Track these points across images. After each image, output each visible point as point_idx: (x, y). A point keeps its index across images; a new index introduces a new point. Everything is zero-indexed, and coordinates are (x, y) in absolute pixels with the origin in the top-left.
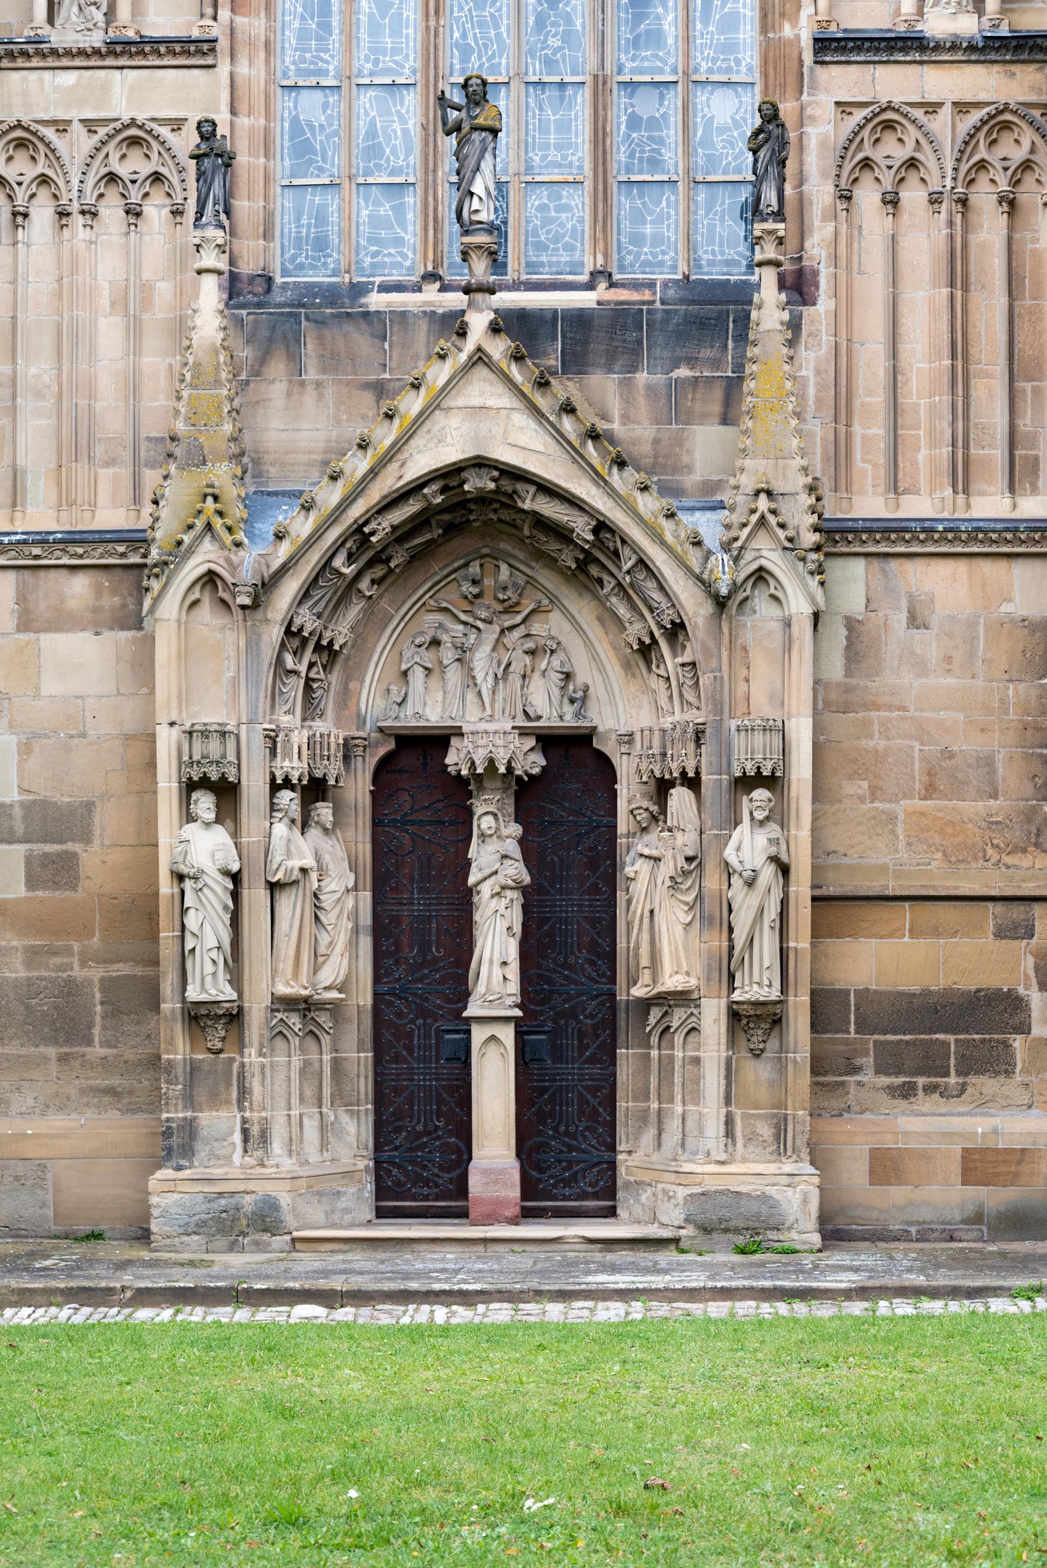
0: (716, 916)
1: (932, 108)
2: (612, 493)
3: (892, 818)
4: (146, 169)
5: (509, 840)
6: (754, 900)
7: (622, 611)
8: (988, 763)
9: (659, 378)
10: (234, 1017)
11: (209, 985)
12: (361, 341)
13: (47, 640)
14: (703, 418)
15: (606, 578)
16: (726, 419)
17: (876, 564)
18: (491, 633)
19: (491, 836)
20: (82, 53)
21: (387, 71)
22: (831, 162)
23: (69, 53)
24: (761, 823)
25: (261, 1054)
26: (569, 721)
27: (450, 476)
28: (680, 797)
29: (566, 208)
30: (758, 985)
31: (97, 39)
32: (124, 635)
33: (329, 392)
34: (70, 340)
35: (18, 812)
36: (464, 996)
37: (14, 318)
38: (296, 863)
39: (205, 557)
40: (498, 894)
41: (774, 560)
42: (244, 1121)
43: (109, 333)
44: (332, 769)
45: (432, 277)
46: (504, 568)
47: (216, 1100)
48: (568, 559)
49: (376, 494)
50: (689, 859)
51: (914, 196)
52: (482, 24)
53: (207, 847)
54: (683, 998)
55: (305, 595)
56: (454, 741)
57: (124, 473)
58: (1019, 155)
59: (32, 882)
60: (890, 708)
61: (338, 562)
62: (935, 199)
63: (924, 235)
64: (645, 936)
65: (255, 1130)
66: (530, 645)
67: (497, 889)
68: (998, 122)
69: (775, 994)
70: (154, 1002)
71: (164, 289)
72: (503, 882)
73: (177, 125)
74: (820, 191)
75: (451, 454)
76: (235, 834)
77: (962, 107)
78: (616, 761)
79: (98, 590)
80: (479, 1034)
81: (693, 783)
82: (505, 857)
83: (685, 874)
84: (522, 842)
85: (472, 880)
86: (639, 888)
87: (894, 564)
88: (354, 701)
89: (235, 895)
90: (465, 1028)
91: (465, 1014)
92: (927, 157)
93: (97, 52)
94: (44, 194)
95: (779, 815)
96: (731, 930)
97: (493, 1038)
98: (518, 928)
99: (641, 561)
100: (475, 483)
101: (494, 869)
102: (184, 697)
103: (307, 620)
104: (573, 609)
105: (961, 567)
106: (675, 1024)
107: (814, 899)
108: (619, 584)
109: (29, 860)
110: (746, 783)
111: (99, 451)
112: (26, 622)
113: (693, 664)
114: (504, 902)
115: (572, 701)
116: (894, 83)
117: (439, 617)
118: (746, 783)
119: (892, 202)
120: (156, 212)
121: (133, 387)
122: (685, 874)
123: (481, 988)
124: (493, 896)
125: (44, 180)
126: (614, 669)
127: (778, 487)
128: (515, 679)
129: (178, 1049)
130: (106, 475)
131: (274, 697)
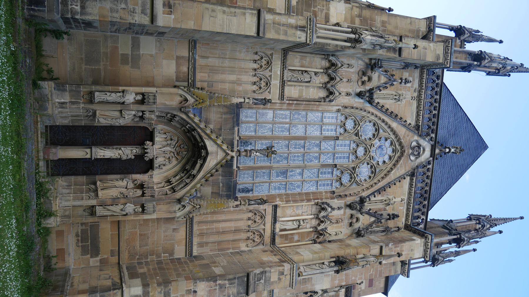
0: (115, 201)
1: (264, 225)
2: (201, 179)
3: (135, 228)
4: (262, 86)
6: (118, 211)
7: (177, 178)
8: (147, 245)
9: (220, 181)
10: (91, 101)
11: (98, 97)
12: (229, 126)
13: (174, 62)
14: (212, 189)
15: (184, 174)
16: (212, 193)
17: (185, 222)
18: (173, 150)
20: (283, 76)
21: (275, 129)
22: (256, 209)
23: (283, 73)
24: (134, 210)
25: (82, 107)
26: (156, 165)
27: (205, 147)
28: (139, 192)
29: (250, 161)
30: (100, 211)
31: (285, 79)
32: (175, 77)
33: (220, 120)
34: (232, 70)
35: (138, 53)
37: (236, 59)
38: (126, 116)
39: (191, 100)
41: (188, 209)
42: (66, 103)
43: (233, 77)
44: (146, 121)
45: (240, 138)
46: (186, 153)
47: (71, 96)
48: (188, 167)
49: (203, 134)
50: (127, 196)
51: (250, 222)
52: (282, 146)
53: (130, 98)
54: (97, 195)
55: (182, 119)
56: (151, 143)
57: (207, 79)
58: (256, 240)
59: (123, 55)
60: (157, 227)
61: (189, 125)
62: (249, 226)
63: (243, 225)
64: (110, 185)
65: (64, 106)
66: (171, 158)
68: (261, 236)
69: (97, 215)
70: (96, 82)
71: (241, 88)
73: (269, 92)
74: (251, 207)
75: (209, 148)
76: (132, 103)
77: (264, 230)
78: (147, 174)
79: (184, 73)
80: (88, 150)
81: (143, 195)
83: (124, 195)
84: (131, 159)
86: (120, 183)
87: (185, 225)
89: (119, 103)
92: (257, 224)
93: (283, 79)
94: (259, 66)
95: (136, 213)
96: (112, 205)
99: (187, 184)
100: (203, 153)
102: (162, 93)
103: (177, 119)
104: (178, 166)
105: (185, 237)
106: (91, 194)
107: (119, 221)
108: (182, 177)
109: (128, 54)
110: (143, 207)
111: (211, 74)
112: (178, 58)
113: (167, 194)
114: (117, 155)
116: (269, 219)
117: (176, 140)
118: (143, 207)
119: (249, 219)
120: (255, 88)
121: (223, 82)
122: (124, 195)
123: (99, 150)
125: (261, 66)
126: (165, 174)
127: (201, 209)
128: (164, 155)
129: (83, 89)
130: (206, 75)
131: (162, 112)
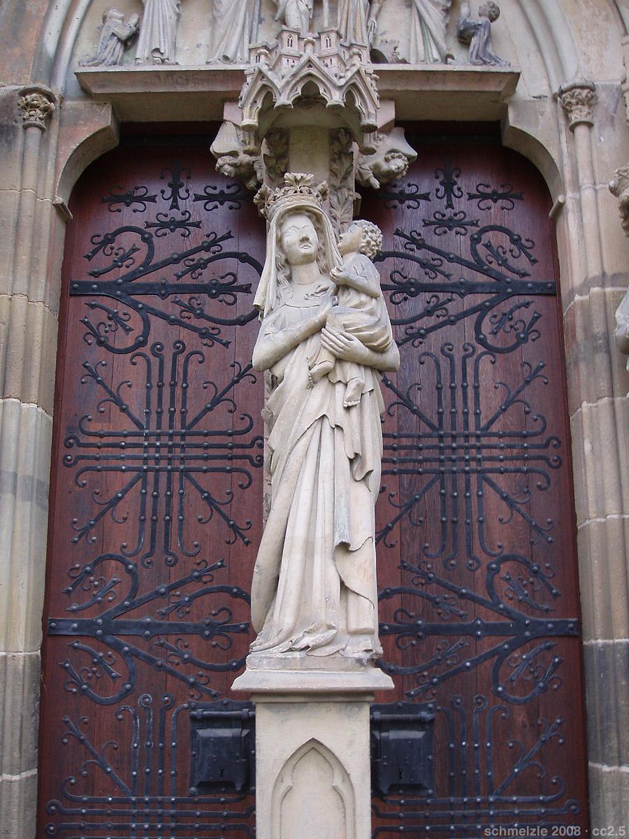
5: (352, 257)
19: (308, 259)
26: (462, 62)
36: (235, 636)
40: (326, 374)
67: (326, 361)
72: (341, 342)
80: (275, 739)
82: (343, 286)
85: (262, 350)
88: (33, 32)
90: (242, 716)
91: (239, 684)
97: (314, 746)
98: (373, 461)
101: (316, 319)
115: (464, 38)
123: (283, 615)
124: (312, 383)
